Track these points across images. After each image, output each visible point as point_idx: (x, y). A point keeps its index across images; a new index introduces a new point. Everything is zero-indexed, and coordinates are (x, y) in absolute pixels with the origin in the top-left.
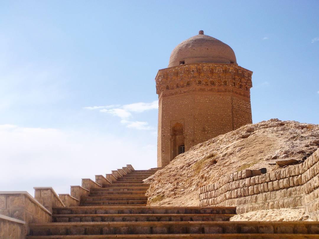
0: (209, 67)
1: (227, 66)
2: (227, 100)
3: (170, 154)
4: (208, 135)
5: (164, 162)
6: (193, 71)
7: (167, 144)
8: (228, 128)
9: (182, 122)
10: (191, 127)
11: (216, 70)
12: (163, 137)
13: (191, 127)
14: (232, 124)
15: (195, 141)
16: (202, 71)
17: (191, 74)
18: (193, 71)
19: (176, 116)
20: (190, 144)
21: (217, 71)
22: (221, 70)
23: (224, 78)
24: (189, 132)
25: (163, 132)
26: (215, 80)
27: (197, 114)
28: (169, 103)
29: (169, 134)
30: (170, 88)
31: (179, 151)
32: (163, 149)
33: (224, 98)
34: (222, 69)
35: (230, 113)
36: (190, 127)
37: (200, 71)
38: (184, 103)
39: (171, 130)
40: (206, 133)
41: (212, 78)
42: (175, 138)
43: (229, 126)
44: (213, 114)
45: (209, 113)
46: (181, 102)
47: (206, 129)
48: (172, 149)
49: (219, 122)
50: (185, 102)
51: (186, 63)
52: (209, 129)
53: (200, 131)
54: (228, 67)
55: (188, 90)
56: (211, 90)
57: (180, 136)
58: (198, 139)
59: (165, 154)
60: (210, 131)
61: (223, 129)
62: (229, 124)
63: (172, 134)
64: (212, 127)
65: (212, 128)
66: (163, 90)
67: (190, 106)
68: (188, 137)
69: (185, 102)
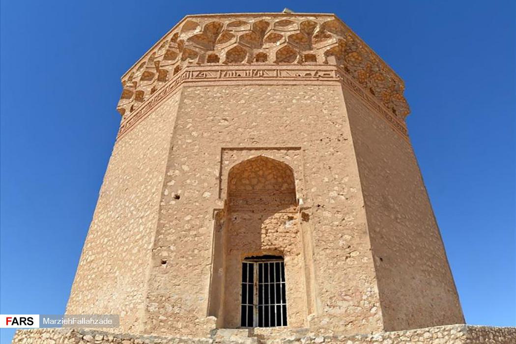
7: (193, 233)
9: (287, 157)
12: (173, 202)
19: (255, 133)
20: (341, 243)
24: (333, 194)
25: (172, 183)
28: (219, 95)
32: (165, 254)
36: (337, 176)
38: (294, 101)
39: (225, 178)
50: (298, 100)
55: (313, 73)
68: (327, 214)
69: (298, 100)
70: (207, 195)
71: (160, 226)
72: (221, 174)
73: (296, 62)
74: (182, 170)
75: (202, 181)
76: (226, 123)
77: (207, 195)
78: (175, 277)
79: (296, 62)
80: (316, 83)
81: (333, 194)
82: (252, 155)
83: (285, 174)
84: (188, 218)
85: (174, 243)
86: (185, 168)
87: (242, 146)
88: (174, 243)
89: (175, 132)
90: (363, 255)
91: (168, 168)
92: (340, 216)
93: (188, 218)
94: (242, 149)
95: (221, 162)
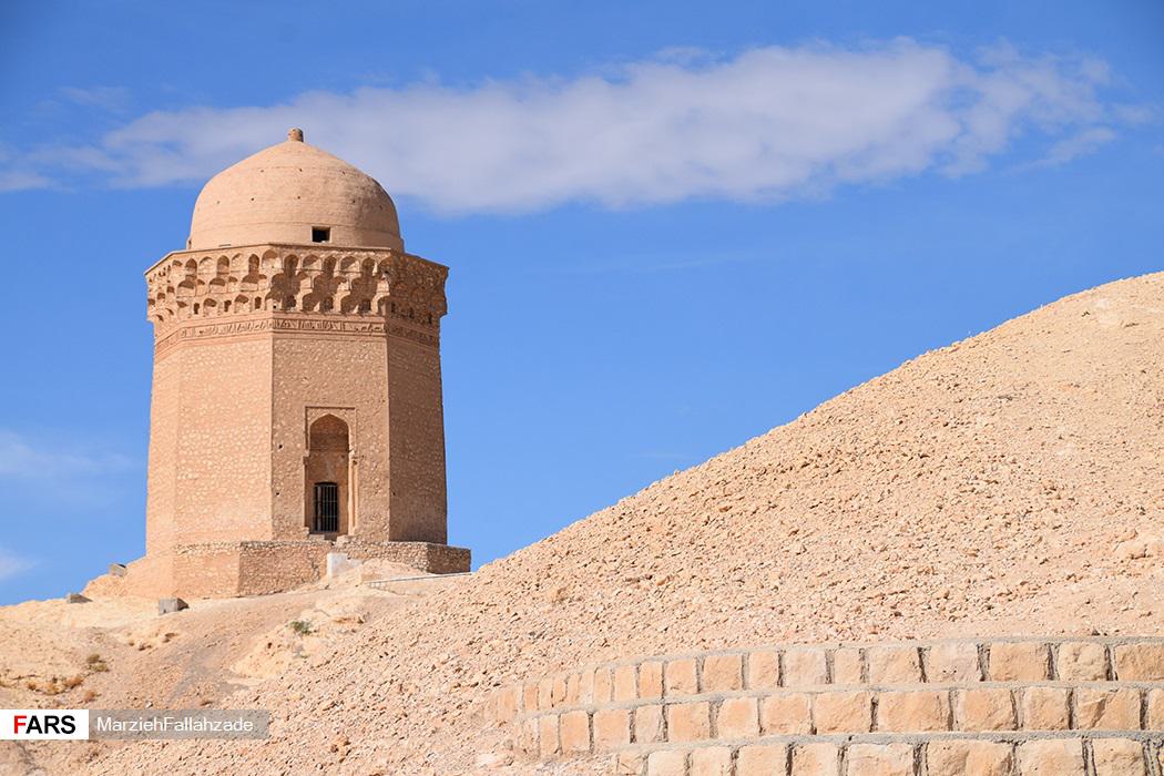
24: (372, 448)
25: (276, 435)
50: (356, 359)
67: (373, 372)
68: (367, 463)
70: (299, 445)
71: (273, 469)
72: (306, 428)
73: (355, 311)
75: (295, 435)
76: (306, 382)
77: (299, 445)
78: (286, 503)
79: (355, 311)
80: (369, 339)
81: (372, 448)
82: (324, 413)
83: (342, 426)
84: (289, 463)
85: (282, 480)
86: (284, 423)
87: (318, 405)
88: (282, 480)
89: (273, 390)
90: (385, 494)
91: (273, 422)
92: (374, 465)
94: (318, 408)
95: (306, 419)
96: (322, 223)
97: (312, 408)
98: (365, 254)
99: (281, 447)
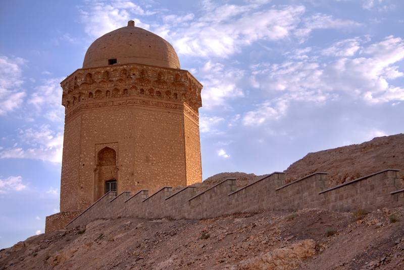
0: (155, 71)
1: (179, 72)
2: (178, 120)
3: (93, 193)
4: (152, 167)
5: (82, 204)
6: (134, 74)
7: (88, 177)
8: (178, 160)
10: (130, 155)
11: (164, 77)
13: (130, 155)
14: (184, 155)
15: (135, 175)
16: (146, 75)
17: (132, 78)
18: (134, 74)
21: (166, 78)
22: (171, 77)
23: (174, 89)
25: (82, 160)
26: (163, 91)
27: (138, 136)
28: (93, 118)
29: (92, 163)
30: (94, 97)
31: (105, 189)
32: (82, 185)
33: (174, 116)
34: (172, 76)
35: (181, 138)
37: (144, 76)
40: (150, 164)
41: (159, 88)
42: (101, 170)
43: (180, 156)
44: (160, 138)
45: (154, 137)
46: (112, 118)
47: (150, 159)
48: (96, 186)
49: (167, 150)
51: (119, 62)
52: (154, 159)
53: (142, 161)
54: (180, 75)
55: (125, 101)
56: (157, 105)
57: (108, 167)
58: (139, 172)
59: (85, 192)
60: (155, 162)
61: (173, 160)
62: (181, 155)
63: (96, 163)
64: (158, 157)
65: (157, 158)
66: (83, 99)
67: (127, 124)
68: (123, 168)
74: (84, 154)
75: (90, 158)
76: (96, 133)
77: (92, 163)
84: (87, 172)
93: (87, 172)
96: (112, 57)
97: (98, 144)
98: (122, 67)
99: (84, 165)
